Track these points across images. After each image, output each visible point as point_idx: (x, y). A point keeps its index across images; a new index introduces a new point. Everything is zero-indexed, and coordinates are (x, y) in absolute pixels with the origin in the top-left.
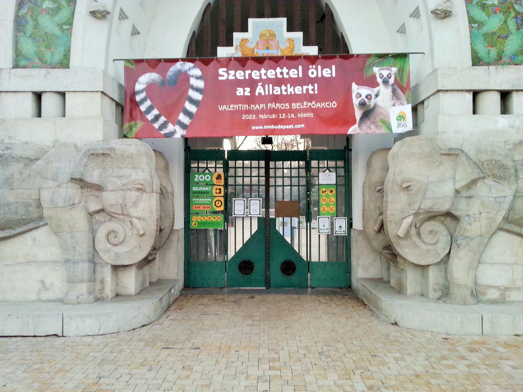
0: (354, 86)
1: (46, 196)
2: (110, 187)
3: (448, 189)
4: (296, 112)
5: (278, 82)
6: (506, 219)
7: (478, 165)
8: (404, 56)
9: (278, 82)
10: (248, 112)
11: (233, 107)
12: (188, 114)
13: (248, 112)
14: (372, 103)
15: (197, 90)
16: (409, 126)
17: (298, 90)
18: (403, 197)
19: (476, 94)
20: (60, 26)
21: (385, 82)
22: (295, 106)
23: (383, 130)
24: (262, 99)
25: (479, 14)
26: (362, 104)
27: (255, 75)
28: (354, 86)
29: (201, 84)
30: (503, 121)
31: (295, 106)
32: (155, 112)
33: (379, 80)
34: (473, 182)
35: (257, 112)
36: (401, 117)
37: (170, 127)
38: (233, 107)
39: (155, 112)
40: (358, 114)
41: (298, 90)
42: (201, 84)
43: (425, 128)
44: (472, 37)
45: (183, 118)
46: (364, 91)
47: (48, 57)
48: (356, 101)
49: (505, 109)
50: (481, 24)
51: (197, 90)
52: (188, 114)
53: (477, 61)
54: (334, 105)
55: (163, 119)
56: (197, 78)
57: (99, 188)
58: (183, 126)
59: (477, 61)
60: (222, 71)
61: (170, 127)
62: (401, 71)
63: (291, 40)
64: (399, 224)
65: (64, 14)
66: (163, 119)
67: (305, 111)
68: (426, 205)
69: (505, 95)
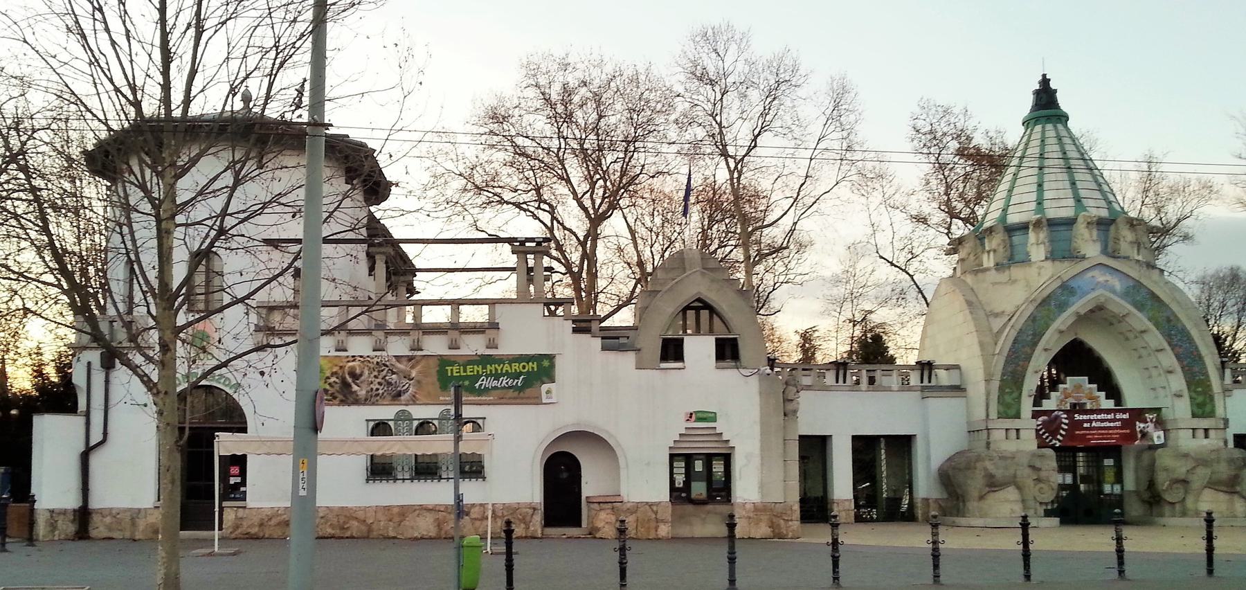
0: (1137, 423)
1: (1019, 473)
2: (1043, 469)
3: (1184, 470)
4: (1111, 434)
5: (1102, 421)
6: (1208, 482)
7: (1196, 460)
8: (1160, 409)
9: (1102, 421)
10: (1089, 434)
11: (1082, 432)
12: (1061, 435)
13: (1089, 434)
14: (1146, 430)
15: (1065, 424)
16: (1162, 441)
17: (1112, 424)
18: (1165, 473)
19: (1193, 429)
20: (1014, 399)
21: (1151, 421)
22: (1111, 432)
23: (1150, 443)
24: (1095, 428)
25: (1194, 395)
26: (1141, 431)
27: (1092, 417)
28: (1137, 423)
29: (1067, 421)
30: (1206, 442)
31: (1111, 432)
32: (1047, 434)
33: (1148, 420)
34: (1194, 468)
35: (1093, 434)
36: (1159, 437)
37: (1054, 442)
38: (1082, 432)
39: (1047, 434)
40: (1139, 436)
41: (1112, 424)
42: (1067, 421)
43: (1170, 443)
44: (1192, 405)
45: (1059, 437)
46: (1142, 425)
47: (1009, 412)
48: (1138, 430)
49: (1207, 437)
50: (1195, 399)
51: (1065, 424)
52: (1061, 435)
53: (1194, 415)
54: (1128, 431)
55: (1050, 438)
56: (1066, 419)
57: (1039, 469)
58: (1060, 441)
59: (1194, 415)
60: (1076, 415)
61: (1054, 442)
62: (1158, 415)
63: (1090, 388)
64: (1163, 485)
65: (1015, 395)
66: (1050, 438)
67: (1116, 434)
68: (1176, 476)
69: (1206, 430)
